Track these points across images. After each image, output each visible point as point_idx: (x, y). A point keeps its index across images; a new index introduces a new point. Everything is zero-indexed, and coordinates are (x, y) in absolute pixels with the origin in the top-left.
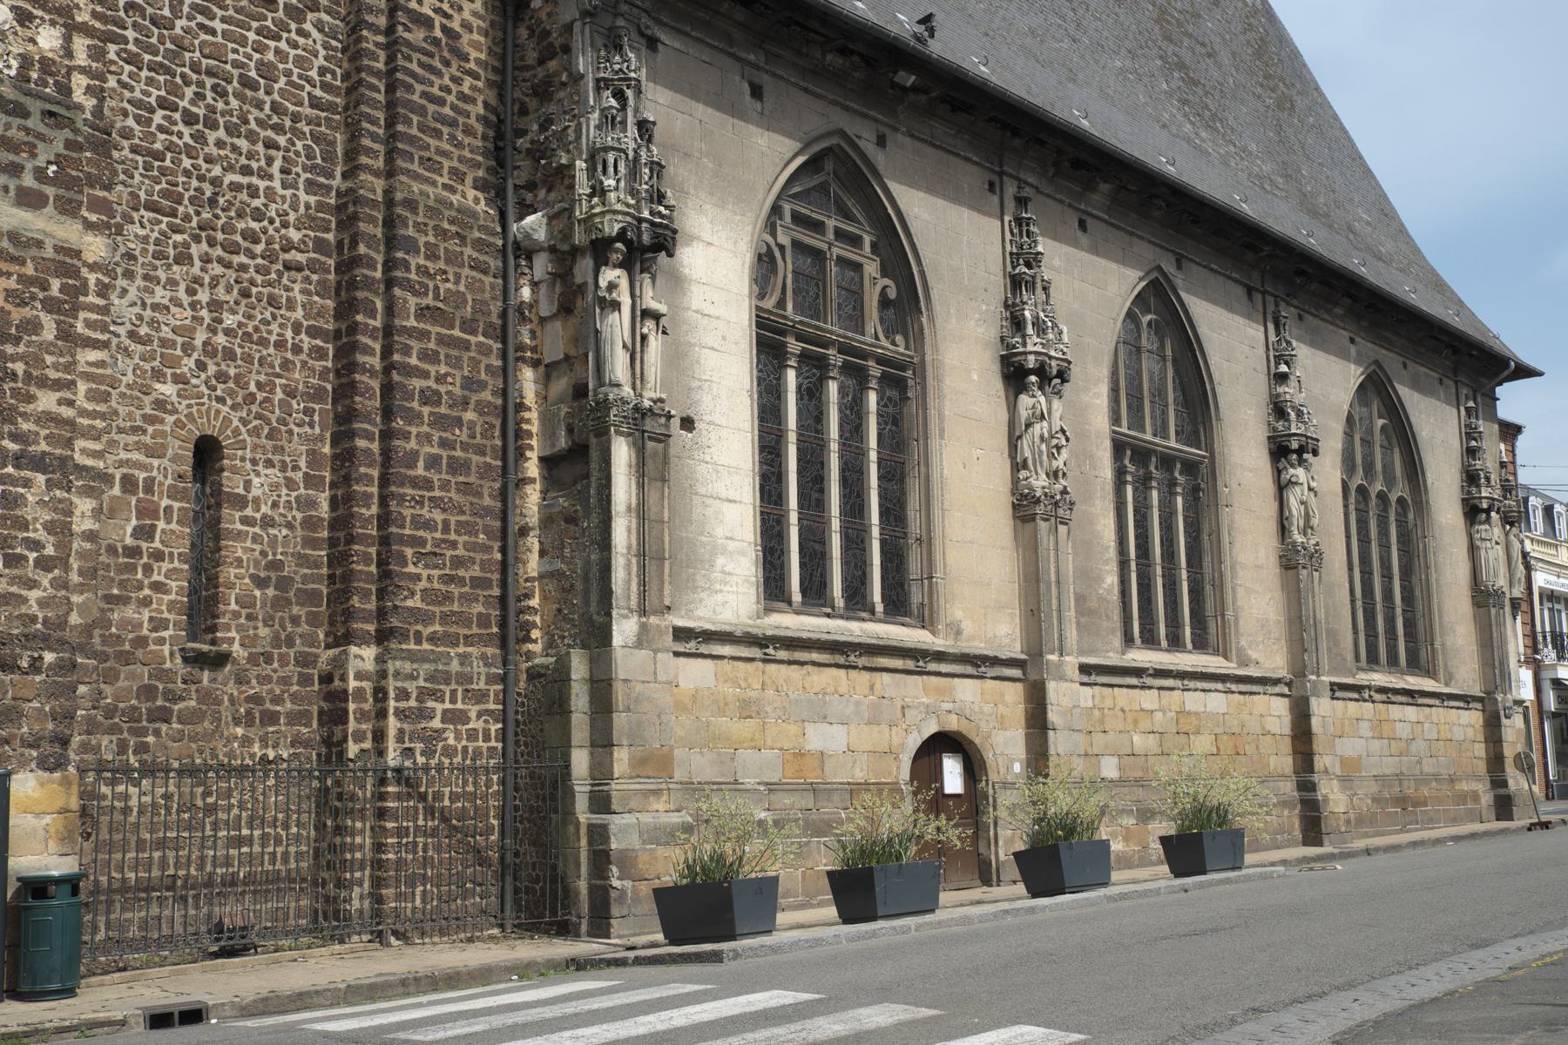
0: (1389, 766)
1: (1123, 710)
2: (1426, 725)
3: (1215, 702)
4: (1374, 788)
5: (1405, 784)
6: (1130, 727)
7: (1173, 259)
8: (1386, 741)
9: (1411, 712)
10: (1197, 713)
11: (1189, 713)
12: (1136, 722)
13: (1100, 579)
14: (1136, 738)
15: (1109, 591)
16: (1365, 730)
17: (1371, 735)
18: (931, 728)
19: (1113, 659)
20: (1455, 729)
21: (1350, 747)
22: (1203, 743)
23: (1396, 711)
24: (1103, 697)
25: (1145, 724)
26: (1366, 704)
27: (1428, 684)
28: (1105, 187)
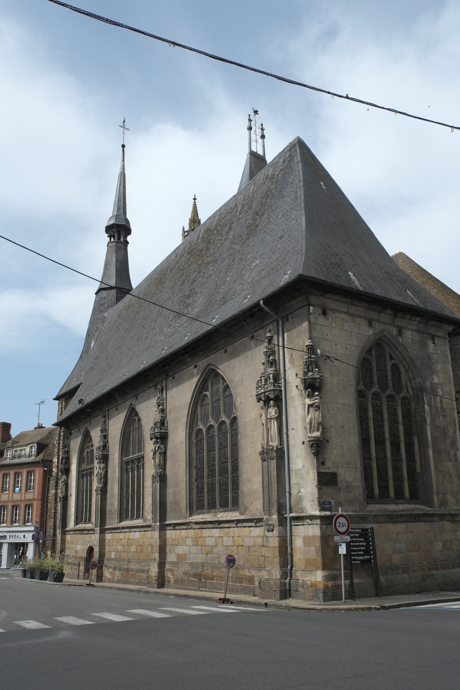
0: (200, 558)
1: (116, 539)
2: (225, 538)
3: (136, 535)
4: (188, 569)
5: (206, 568)
6: (117, 544)
7: (135, 398)
8: (200, 547)
9: (216, 532)
10: (132, 539)
11: (130, 539)
12: (119, 543)
13: (115, 504)
14: (118, 547)
15: (116, 507)
16: (189, 542)
17: (192, 544)
18: (88, 546)
19: (115, 525)
20: (246, 540)
21: (181, 550)
22: (133, 549)
23: (206, 532)
24: (113, 536)
25: (120, 544)
26: (191, 530)
27: (234, 515)
28: (117, 396)
